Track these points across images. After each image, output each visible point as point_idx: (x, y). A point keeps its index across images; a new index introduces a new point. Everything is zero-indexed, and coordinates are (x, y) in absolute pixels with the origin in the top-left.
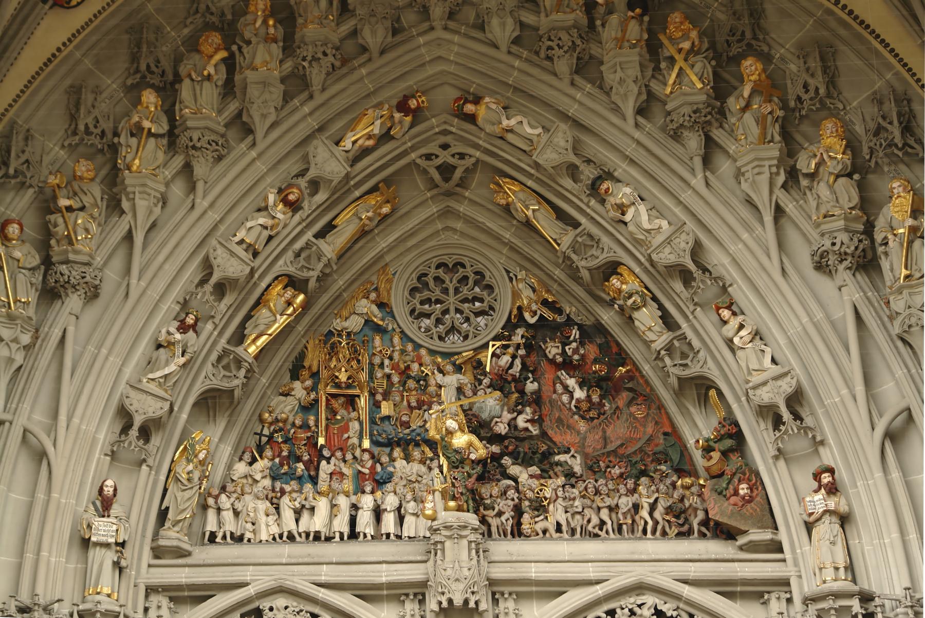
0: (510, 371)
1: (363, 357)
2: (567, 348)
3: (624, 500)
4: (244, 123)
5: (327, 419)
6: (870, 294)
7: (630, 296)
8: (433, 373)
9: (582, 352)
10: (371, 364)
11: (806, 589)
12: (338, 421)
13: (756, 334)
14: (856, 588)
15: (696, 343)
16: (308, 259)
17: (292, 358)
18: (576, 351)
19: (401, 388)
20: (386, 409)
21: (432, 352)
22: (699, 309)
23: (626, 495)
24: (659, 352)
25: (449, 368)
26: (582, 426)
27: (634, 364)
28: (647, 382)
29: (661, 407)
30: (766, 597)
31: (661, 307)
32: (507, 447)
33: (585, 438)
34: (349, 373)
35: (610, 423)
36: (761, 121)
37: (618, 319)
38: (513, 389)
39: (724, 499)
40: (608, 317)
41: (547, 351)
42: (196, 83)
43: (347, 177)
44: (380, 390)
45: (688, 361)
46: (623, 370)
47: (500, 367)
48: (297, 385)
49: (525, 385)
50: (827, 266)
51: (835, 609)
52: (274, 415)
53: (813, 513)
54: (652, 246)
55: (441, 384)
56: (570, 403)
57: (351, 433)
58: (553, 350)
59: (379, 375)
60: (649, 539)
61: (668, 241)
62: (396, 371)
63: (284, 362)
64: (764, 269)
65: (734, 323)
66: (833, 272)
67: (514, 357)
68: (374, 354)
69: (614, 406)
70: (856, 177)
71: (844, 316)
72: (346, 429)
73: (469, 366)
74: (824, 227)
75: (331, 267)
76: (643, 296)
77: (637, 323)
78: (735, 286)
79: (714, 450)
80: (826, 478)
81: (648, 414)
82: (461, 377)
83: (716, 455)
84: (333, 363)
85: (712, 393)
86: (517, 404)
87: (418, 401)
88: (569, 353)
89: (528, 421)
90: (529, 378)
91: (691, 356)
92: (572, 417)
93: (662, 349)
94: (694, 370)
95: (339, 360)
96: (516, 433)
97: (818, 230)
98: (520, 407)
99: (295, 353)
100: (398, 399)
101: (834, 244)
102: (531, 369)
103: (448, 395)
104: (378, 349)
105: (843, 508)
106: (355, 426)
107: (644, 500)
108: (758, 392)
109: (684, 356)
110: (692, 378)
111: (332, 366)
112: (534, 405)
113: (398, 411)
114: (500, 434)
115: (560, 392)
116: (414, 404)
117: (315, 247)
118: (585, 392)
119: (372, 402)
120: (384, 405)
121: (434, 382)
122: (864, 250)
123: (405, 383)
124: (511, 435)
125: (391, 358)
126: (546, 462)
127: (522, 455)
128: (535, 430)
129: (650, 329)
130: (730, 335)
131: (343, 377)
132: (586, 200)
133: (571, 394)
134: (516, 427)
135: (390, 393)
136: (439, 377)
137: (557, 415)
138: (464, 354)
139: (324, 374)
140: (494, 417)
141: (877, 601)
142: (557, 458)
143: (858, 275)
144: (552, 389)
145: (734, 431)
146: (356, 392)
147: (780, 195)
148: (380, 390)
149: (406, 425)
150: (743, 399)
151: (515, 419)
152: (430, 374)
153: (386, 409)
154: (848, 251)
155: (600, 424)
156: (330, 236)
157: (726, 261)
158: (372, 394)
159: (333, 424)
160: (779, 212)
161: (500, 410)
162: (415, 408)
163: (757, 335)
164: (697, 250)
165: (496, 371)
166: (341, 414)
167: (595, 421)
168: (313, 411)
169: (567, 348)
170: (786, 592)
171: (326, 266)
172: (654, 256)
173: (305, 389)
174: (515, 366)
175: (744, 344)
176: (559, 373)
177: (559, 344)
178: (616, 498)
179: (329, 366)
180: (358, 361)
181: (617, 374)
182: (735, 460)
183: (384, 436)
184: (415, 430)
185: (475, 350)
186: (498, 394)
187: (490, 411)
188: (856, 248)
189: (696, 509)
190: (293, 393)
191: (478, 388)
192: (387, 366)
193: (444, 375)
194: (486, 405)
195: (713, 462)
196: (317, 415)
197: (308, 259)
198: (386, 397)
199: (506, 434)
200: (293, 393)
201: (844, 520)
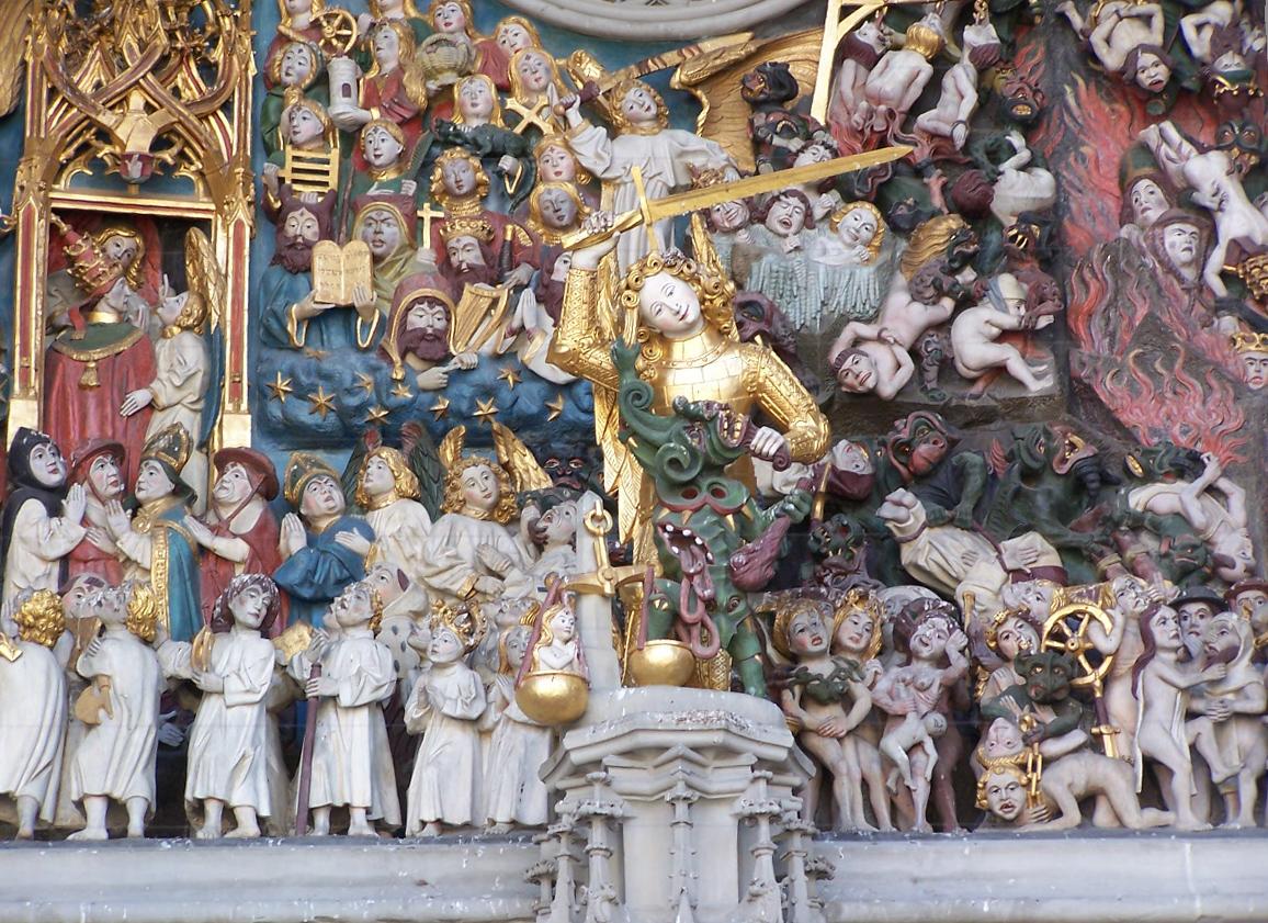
0: (925, 119)
2: (1188, 23)
5: (52, 327)
9: (1258, 45)
10: (270, 84)
18: (1226, 38)
19: (410, 187)
25: (637, 100)
32: (904, 449)
34: (161, 118)
38: (937, 201)
41: (1097, 38)
44: (309, 194)
47: (879, 99)
55: (599, 170)
56: (1201, 262)
57: (163, 389)
59: (307, 122)
62: (386, 111)
67: (941, 61)
68: (283, 40)
72: (145, 372)
73: (730, 97)
84: (88, 79)
87: (486, 245)
88: (1200, 45)
89: (1005, 336)
90: (1013, 151)
92: (1207, 324)
95: (114, 61)
96: (950, 393)
98: (968, 275)
100: (394, 232)
102: (1023, 111)
104: (304, 20)
106: (181, 357)
111: (86, 86)
112: (1030, 267)
113: (390, 289)
114: (873, 393)
115: (1154, 215)
116: (469, 257)
119: (266, 252)
120: (326, 256)
121: (565, 165)
123: (428, 165)
124: (921, 398)
125: (363, 58)
126: (1087, 515)
127: (975, 482)
128: (1035, 378)
131: (135, 132)
133: (1205, 219)
134: (947, 365)
135: (355, 208)
136: (590, 141)
137: (1142, 312)
138: (708, 46)
140: (845, 320)
142: (1138, 498)
144: (1112, 205)
148: (309, 194)
149: (433, 348)
151: (944, 326)
152: (547, 128)
158: (271, 217)
159: (83, 346)
161: (875, 286)
162: (474, 274)
165: (857, 117)
169: (1188, 23)
174: (948, 96)
176: (1151, 134)
180: (208, 70)
183: (322, 398)
184: (470, 370)
185: (756, 28)
186: (864, 215)
187: (830, 290)
192: (346, 90)
193: (613, 132)
194: (808, 264)
198: (336, 218)
199: (900, 392)
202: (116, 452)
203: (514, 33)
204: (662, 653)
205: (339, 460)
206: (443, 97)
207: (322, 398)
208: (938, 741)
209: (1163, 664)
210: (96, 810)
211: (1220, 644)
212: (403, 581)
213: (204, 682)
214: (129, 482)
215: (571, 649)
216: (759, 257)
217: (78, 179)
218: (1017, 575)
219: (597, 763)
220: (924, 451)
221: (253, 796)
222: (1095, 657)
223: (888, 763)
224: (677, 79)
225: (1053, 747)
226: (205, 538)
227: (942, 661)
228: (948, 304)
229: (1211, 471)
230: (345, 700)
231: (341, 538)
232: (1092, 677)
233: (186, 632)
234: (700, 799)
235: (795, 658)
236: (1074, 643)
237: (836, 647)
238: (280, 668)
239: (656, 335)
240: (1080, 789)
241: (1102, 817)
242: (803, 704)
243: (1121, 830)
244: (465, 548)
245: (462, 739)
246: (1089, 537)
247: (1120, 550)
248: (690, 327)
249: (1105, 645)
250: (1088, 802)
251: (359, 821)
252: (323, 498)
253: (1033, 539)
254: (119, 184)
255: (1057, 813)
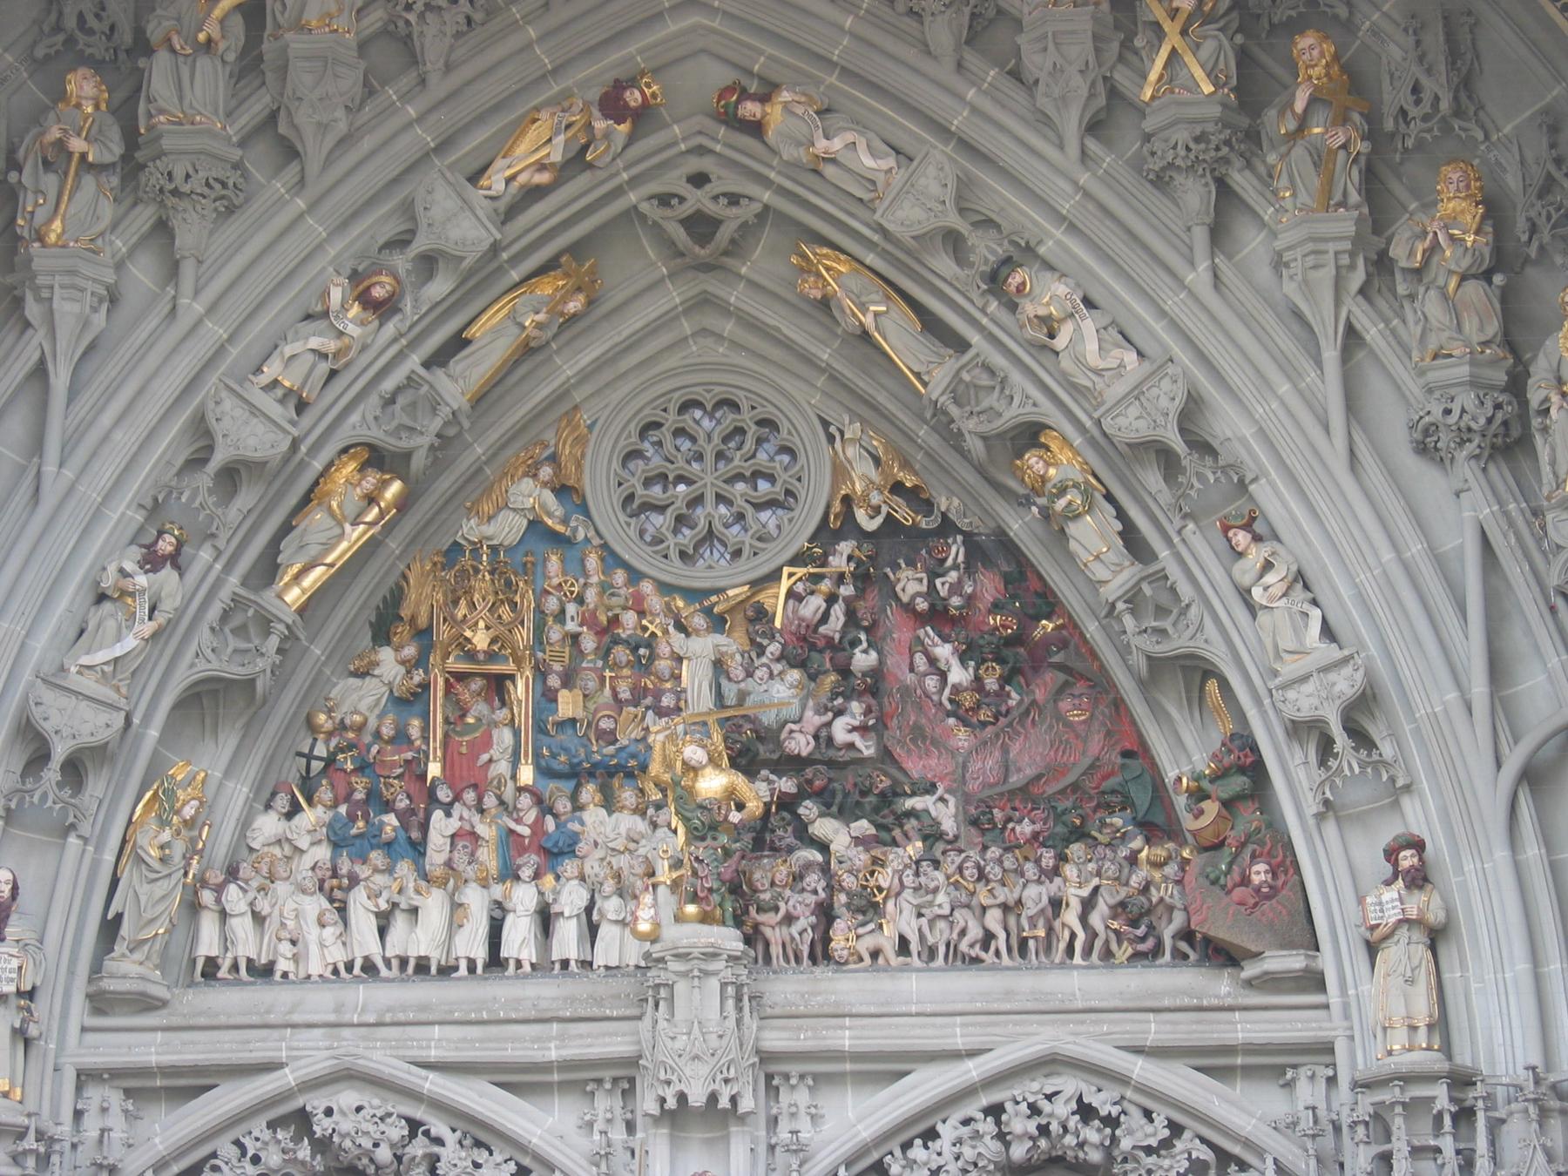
0: (822, 629)
1: (522, 597)
2: (938, 582)
3: (1032, 891)
4: (283, 138)
5: (446, 721)
6: (1512, 506)
7: (1063, 491)
8: (666, 632)
9: (969, 590)
10: (540, 611)
11: (1361, 1066)
12: (471, 729)
13: (1295, 580)
14: (1445, 1066)
15: (1185, 590)
16: (412, 406)
17: (377, 600)
18: (956, 589)
19: (600, 663)
20: (568, 705)
21: (665, 588)
22: (1191, 526)
23: (1039, 882)
24: (1113, 606)
25: (699, 621)
26: (962, 738)
27: (1070, 617)
28: (1093, 654)
29: (1119, 705)
30: (1289, 1075)
31: (1121, 514)
32: (810, 782)
33: (964, 767)
35: (1019, 734)
36: (1321, 159)
37: (1039, 529)
38: (828, 665)
39: (1222, 894)
40: (1019, 525)
41: (898, 588)
42: (181, 59)
43: (495, 248)
44: (557, 667)
45: (1167, 624)
46: (1049, 626)
48: (386, 654)
49: (851, 657)
50: (1436, 449)
51: (1404, 1104)
52: (337, 716)
53: (1378, 925)
54: (1102, 403)
56: (942, 691)
57: (495, 752)
58: (910, 584)
59: (555, 634)
60: (1077, 967)
61: (1136, 393)
63: (361, 608)
64: (1316, 452)
65: (1256, 555)
66: (1447, 462)
67: (831, 599)
69: (1027, 701)
70: (1498, 279)
71: (1462, 546)
72: (487, 743)
73: (739, 617)
74: (1432, 376)
75: (459, 423)
76: (1087, 494)
77: (1073, 545)
78: (1263, 481)
79: (1208, 797)
80: (1408, 859)
81: (1092, 715)
82: (720, 639)
83: (1211, 808)
84: (462, 610)
85: (1212, 686)
86: (835, 696)
87: (633, 690)
88: (943, 592)
89: (854, 729)
91: (1175, 611)
93: (1119, 598)
94: (1179, 643)
95: (471, 606)
96: (831, 753)
97: (1422, 381)
98: (840, 700)
99: (384, 591)
100: (591, 685)
101: (1448, 412)
102: (866, 623)
103: (696, 680)
104: (555, 581)
105: (1435, 915)
106: (504, 737)
107: (1072, 891)
108: (1291, 694)
109: (1161, 611)
110: (1177, 657)
111: (460, 616)
116: (625, 694)
117: (425, 388)
118: (971, 670)
119: (539, 688)
120: (564, 695)
122: (1505, 423)
123: (608, 652)
124: (818, 756)
125: (580, 600)
126: (886, 811)
129: (1097, 557)
130: (1246, 580)
131: (481, 640)
132: (975, 296)
133: (943, 675)
134: (830, 740)
136: (677, 638)
138: (731, 593)
139: (443, 632)
140: (786, 722)
141: (1480, 1090)
142: (910, 803)
143: (1492, 469)
145: (1249, 760)
146: (509, 667)
147: (1355, 309)
148: (557, 667)
149: (610, 737)
150: (1267, 701)
151: (829, 724)
152: (659, 634)
153: (568, 705)
154: (1474, 425)
155: (997, 736)
156: (457, 363)
157: (1248, 431)
158: (541, 672)
159: (461, 734)
160: (1352, 336)
163: (1300, 578)
164: (1191, 412)
166: (479, 709)
167: (989, 729)
168: (418, 708)
169: (938, 582)
170: (1327, 1066)
171: (446, 424)
172: (1107, 424)
173: (403, 663)
174: (832, 618)
175: (1271, 599)
176: (921, 632)
177: (924, 575)
178: (1018, 889)
179: (453, 617)
180: (513, 605)
181: (1038, 634)
182: (1249, 819)
186: (795, 675)
188: (1490, 421)
189: (1171, 909)
190: (376, 672)
191: (757, 663)
195: (1205, 821)
196: (425, 717)
197: (412, 406)
198: (568, 681)
200: (376, 672)
201: (1436, 937)
202: (475, 786)
203: (647, 587)
204: (691, 909)
205: (568, 786)
206: (615, 621)
207: (563, 758)
208: (813, 928)
209: (907, 894)
210: (463, 965)
211: (932, 885)
212: (596, 844)
213: (508, 905)
214: (480, 799)
215: (652, 911)
216: (749, 694)
217: (457, 658)
218: (858, 841)
219: (662, 960)
220: (817, 783)
221: (529, 954)
222: (880, 889)
223: (793, 939)
224: (716, 610)
225: (861, 931)
226: (513, 825)
227: (815, 892)
228: (830, 714)
229: (940, 792)
230: (567, 914)
231: (570, 825)
232: (879, 898)
233: (502, 879)
234: (707, 974)
235: (755, 891)
236: (872, 883)
237: (773, 884)
238: (541, 893)
239: (692, 769)
240: (872, 947)
241: (881, 960)
242: (758, 911)
243: (888, 968)
244: (623, 830)
245: (616, 929)
246: (890, 820)
247: (901, 826)
248: (704, 767)
249: (885, 885)
250: (875, 954)
251: (573, 963)
252: (563, 805)
253: (864, 823)
254: (478, 662)
255: (861, 959)
